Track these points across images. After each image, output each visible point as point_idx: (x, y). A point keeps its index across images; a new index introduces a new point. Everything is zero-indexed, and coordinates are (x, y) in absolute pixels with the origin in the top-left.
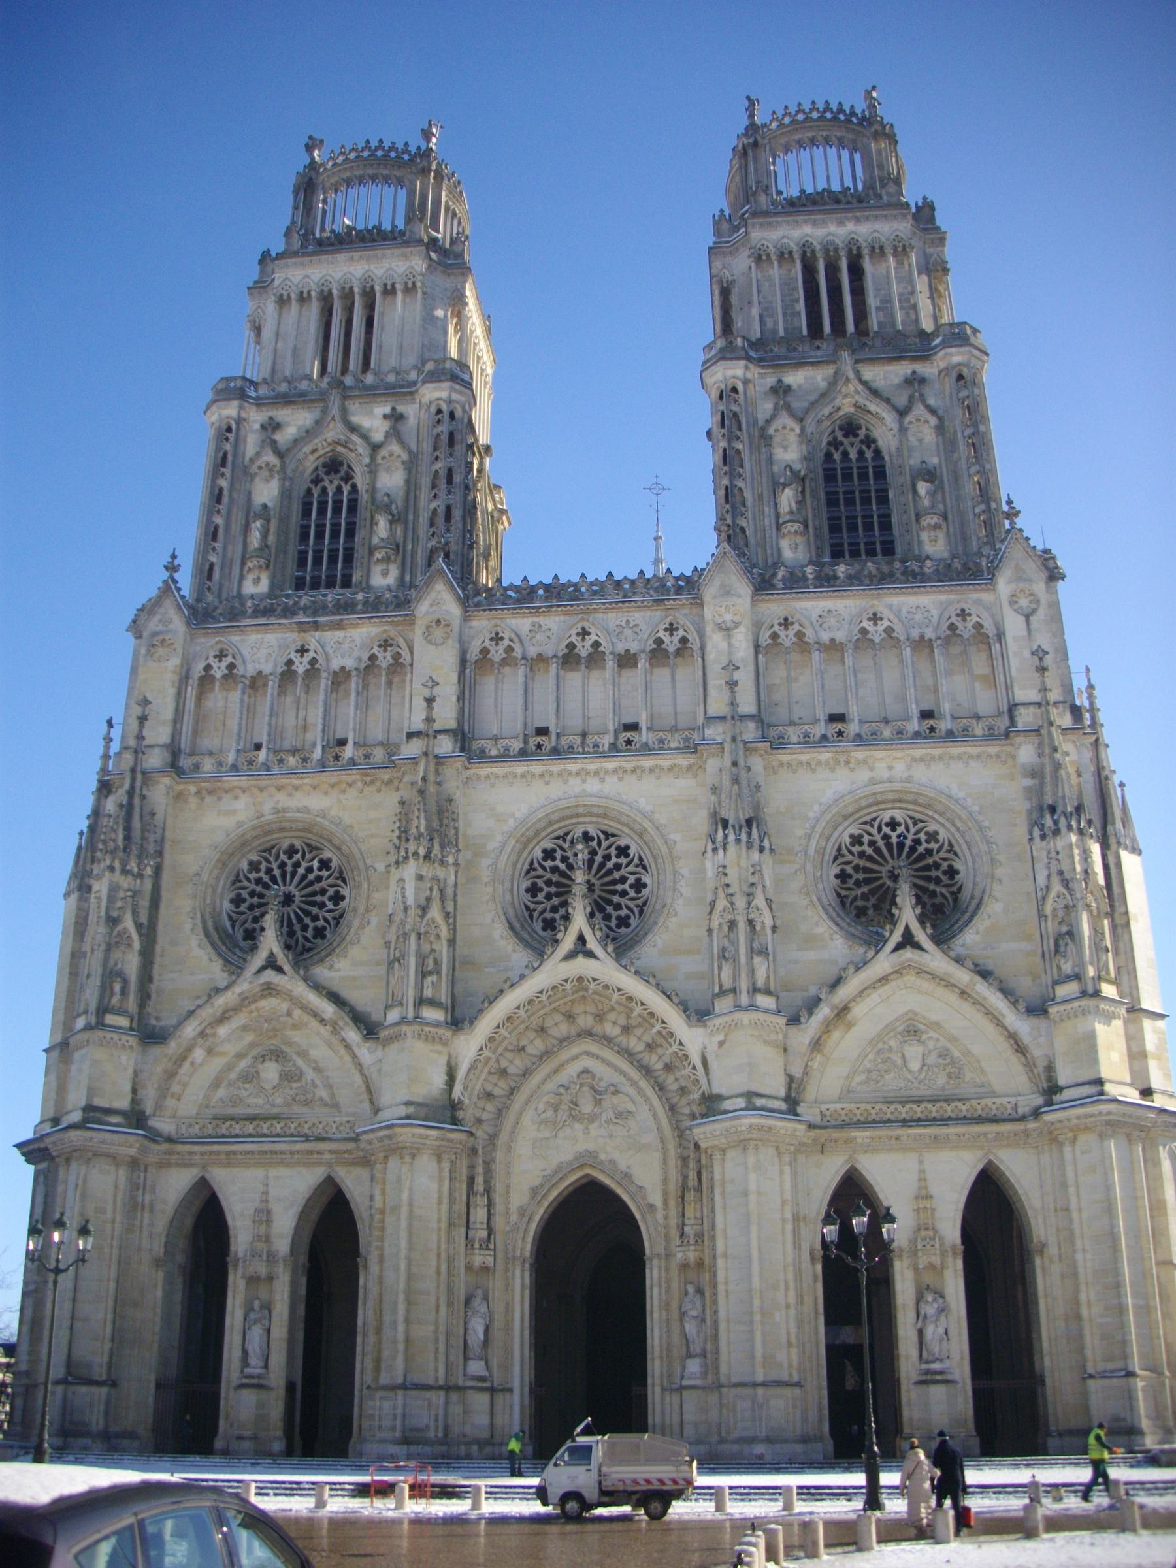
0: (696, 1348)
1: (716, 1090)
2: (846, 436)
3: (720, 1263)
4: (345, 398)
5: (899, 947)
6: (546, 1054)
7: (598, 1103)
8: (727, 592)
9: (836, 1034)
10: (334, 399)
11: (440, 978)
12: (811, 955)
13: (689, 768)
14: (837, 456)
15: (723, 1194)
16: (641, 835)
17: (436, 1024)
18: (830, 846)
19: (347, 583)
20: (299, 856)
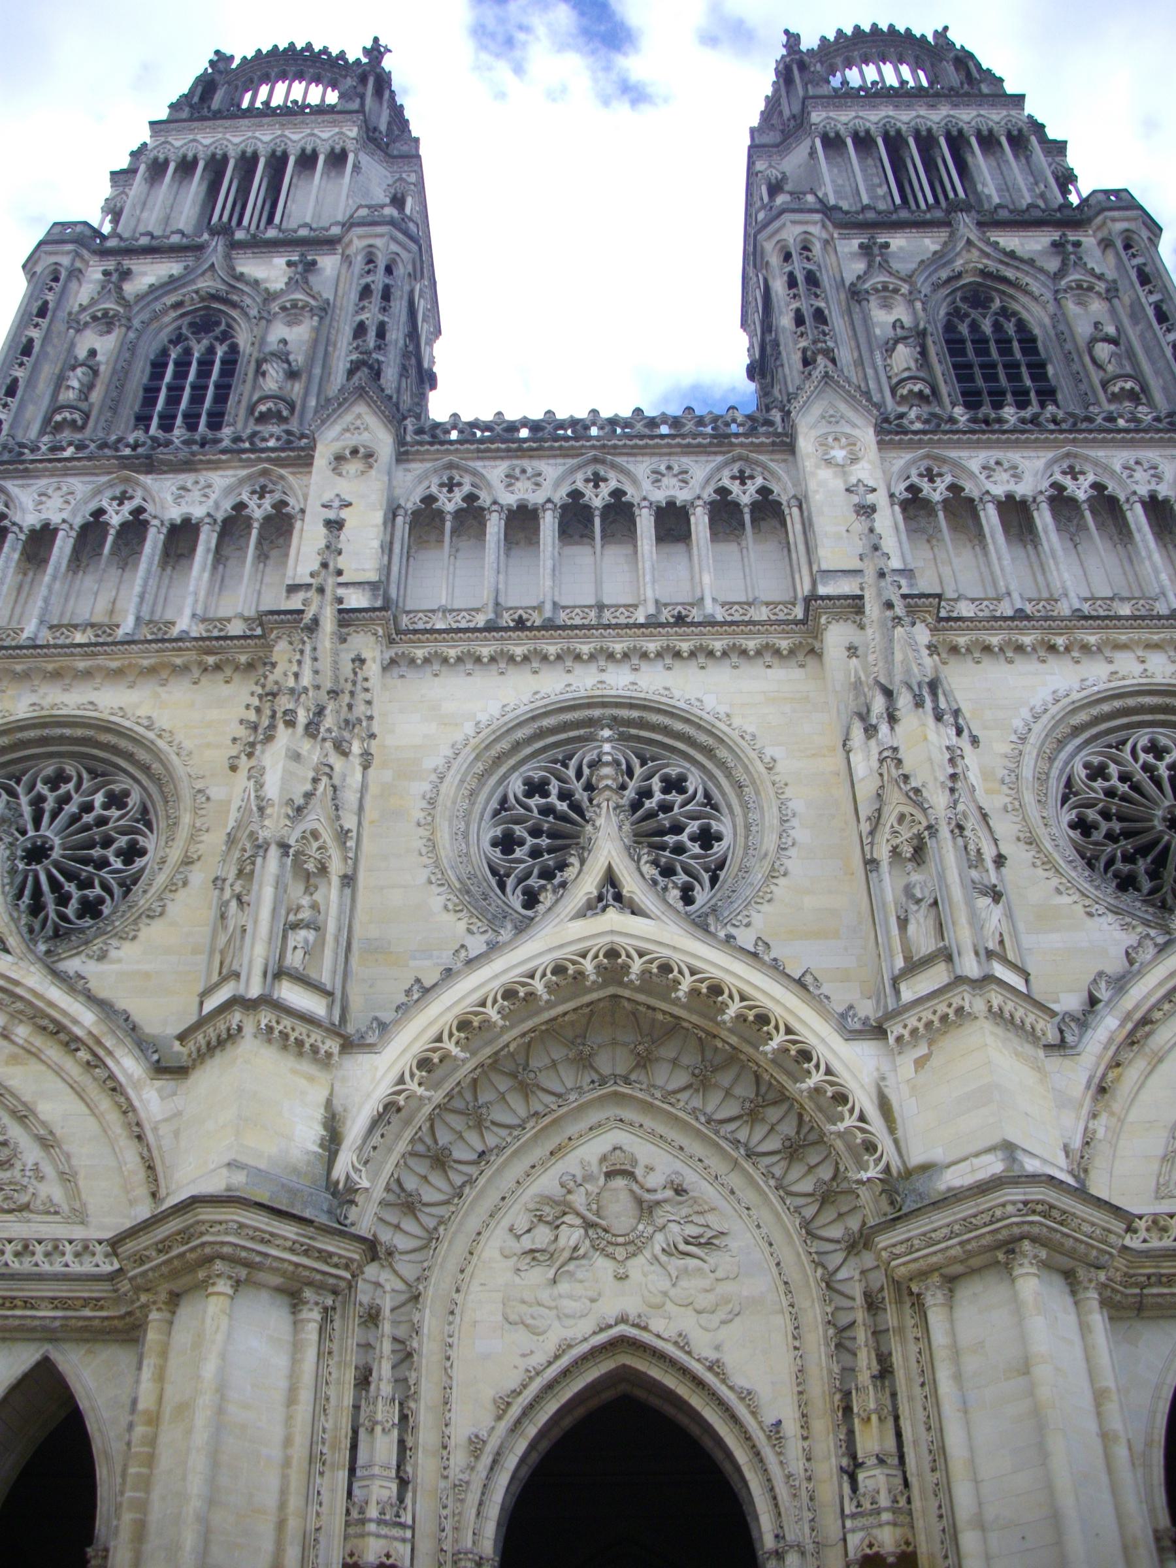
1: (916, 1158)
4: (234, 245)
7: (646, 1208)
9: (1132, 1073)
10: (217, 247)
11: (321, 942)
13: (792, 652)
14: (964, 329)
15: (958, 1377)
16: (708, 752)
17: (307, 1019)
18: (1055, 773)
20: (71, 786)
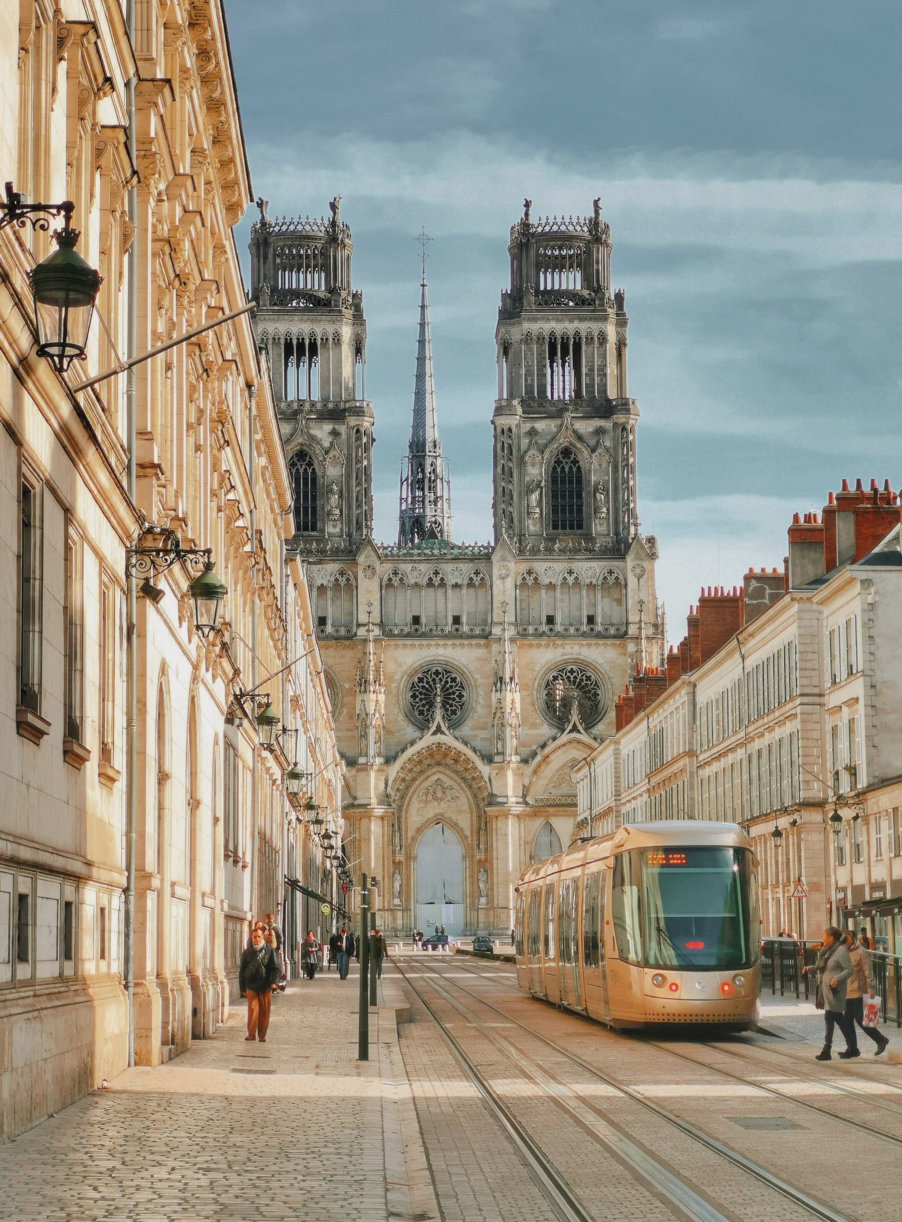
0: (484, 893)
2: (564, 458)
3: (495, 861)
5: (571, 731)
6: (421, 772)
7: (444, 793)
8: (503, 559)
9: (543, 767)
12: (534, 732)
14: (559, 470)
19: (314, 529)
